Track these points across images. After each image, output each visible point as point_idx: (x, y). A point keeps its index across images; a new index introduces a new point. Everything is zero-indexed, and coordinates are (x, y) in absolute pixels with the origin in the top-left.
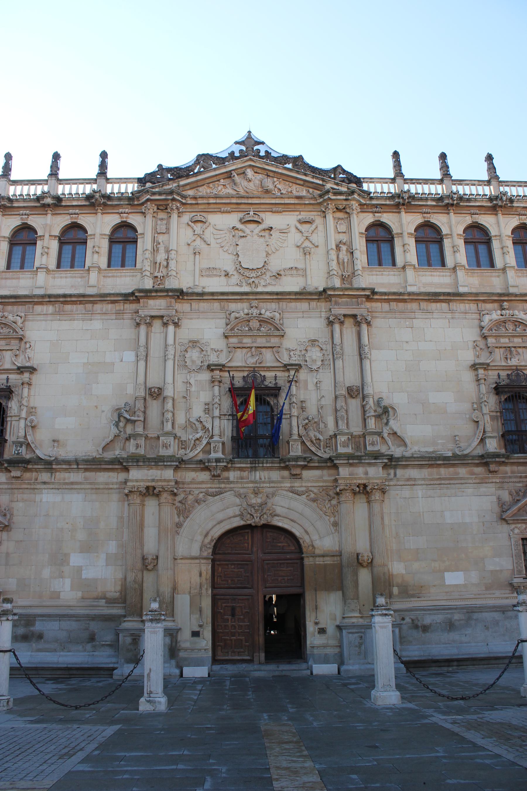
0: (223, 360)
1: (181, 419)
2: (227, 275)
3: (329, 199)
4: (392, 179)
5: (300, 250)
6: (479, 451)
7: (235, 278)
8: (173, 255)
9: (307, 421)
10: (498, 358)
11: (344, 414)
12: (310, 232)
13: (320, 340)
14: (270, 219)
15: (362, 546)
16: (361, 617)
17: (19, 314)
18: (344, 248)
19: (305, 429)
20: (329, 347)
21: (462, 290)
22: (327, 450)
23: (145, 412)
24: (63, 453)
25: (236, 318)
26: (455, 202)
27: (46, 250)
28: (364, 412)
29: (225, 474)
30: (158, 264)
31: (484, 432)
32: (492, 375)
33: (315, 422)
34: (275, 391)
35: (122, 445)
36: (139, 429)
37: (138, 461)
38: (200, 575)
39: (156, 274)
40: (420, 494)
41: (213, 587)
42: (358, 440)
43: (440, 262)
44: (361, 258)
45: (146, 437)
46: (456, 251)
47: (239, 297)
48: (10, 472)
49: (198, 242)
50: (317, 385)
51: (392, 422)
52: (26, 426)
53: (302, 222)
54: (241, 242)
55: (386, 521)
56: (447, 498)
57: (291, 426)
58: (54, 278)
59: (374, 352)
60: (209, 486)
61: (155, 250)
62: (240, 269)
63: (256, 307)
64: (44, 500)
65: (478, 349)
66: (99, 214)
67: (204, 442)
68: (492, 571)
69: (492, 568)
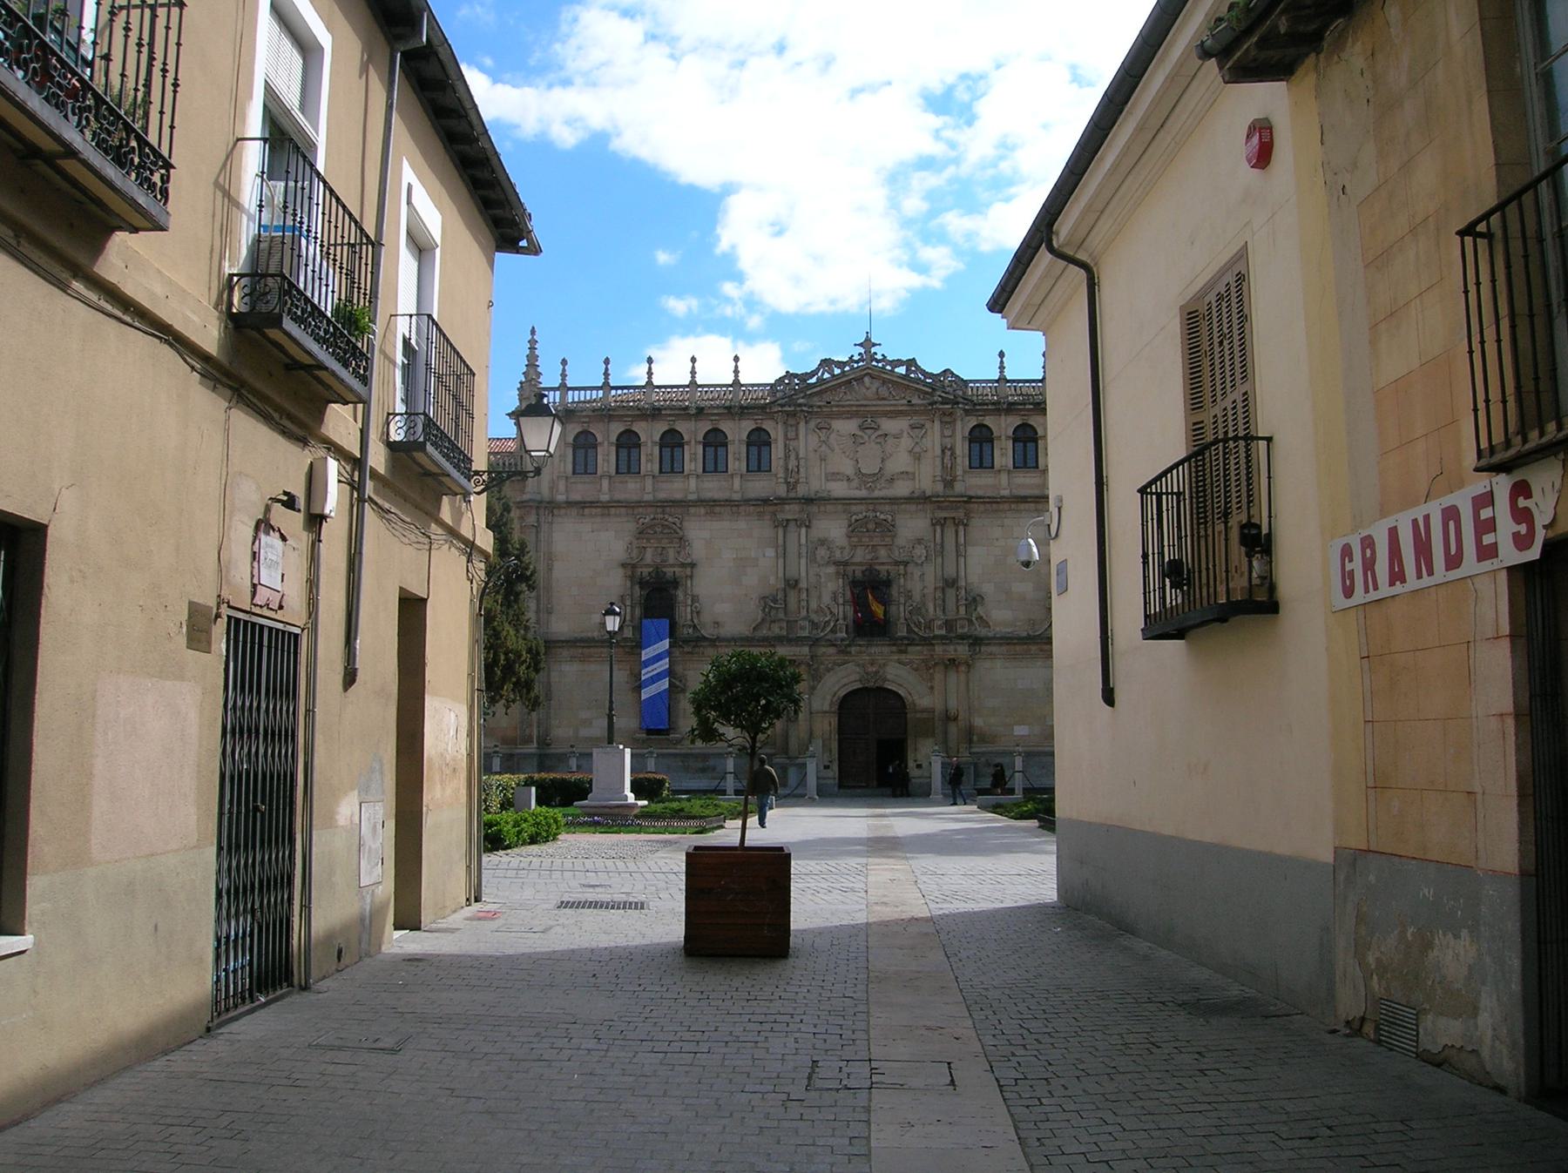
1: (814, 605)
5: (912, 457)
15: (953, 704)
18: (948, 453)
36: (781, 615)
37: (780, 640)
42: (949, 625)
44: (962, 462)
49: (824, 448)
53: (913, 427)
57: (900, 611)
61: (787, 457)
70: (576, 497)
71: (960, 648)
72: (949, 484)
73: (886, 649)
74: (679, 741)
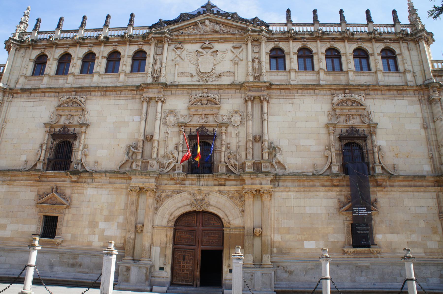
0: (187, 121)
1: (162, 152)
2: (192, 76)
3: (250, 35)
4: (286, 24)
6: (328, 173)
7: (196, 78)
8: (164, 65)
9: (229, 154)
10: (342, 120)
11: (251, 151)
12: (239, 52)
13: (240, 110)
14: (217, 46)
16: (254, 264)
17: (83, 96)
18: (257, 61)
19: (229, 159)
20: (245, 114)
21: (322, 83)
22: (240, 170)
23: (143, 148)
24: (99, 168)
25: (195, 98)
26: (320, 35)
27: (99, 64)
28: (262, 150)
29: (184, 182)
30: (155, 71)
31: (331, 162)
32: (338, 131)
33: (235, 155)
34: (214, 137)
35: (130, 165)
38: (167, 236)
39: (154, 75)
40: (292, 196)
41: (174, 243)
43: (311, 68)
44: (266, 66)
45: (142, 162)
46: (320, 62)
47: (197, 87)
48: (72, 178)
49: (178, 58)
50: (237, 135)
51: (278, 156)
52: (82, 154)
53: (234, 48)
54: (200, 58)
55: (272, 211)
56: (308, 199)
57: (221, 157)
58: (102, 78)
59: (270, 117)
60: (174, 188)
61: (155, 64)
62: (199, 73)
63: (206, 93)
64: (88, 193)
65: (330, 116)
66: (128, 46)
67: (173, 164)
68: (332, 242)
69: (332, 240)
70: (30, 87)
71: (264, 182)
72: (257, 78)
73: (211, 183)
74: (59, 244)
